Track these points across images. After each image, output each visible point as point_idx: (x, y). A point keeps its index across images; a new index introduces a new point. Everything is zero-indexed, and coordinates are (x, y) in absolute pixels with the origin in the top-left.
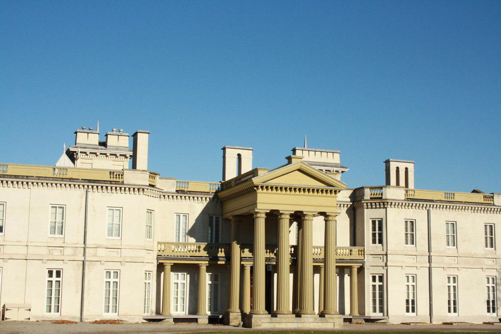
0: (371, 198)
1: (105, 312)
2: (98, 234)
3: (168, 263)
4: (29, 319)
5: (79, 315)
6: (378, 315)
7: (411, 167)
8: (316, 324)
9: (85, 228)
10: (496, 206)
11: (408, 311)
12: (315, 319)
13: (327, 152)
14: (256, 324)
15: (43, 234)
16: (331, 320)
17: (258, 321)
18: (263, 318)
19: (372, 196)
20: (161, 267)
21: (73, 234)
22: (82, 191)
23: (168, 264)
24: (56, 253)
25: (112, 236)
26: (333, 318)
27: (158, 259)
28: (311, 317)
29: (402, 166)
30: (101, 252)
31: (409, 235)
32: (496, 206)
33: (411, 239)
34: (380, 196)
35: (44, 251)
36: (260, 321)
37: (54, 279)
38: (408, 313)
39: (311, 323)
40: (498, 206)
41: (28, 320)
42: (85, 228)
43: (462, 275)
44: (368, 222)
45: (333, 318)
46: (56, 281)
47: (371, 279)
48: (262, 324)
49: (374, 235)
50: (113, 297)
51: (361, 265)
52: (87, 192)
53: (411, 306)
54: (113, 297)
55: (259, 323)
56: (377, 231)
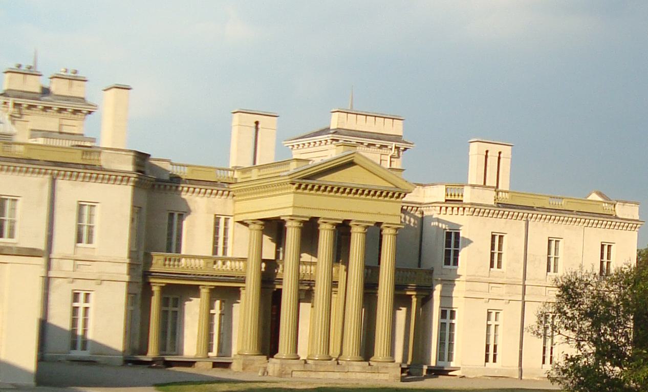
0: (446, 200)
7: (507, 151)
8: (363, 375)
10: (619, 219)
12: (364, 368)
16: (384, 370)
17: (287, 367)
18: (293, 364)
19: (449, 198)
26: (387, 367)
28: (358, 366)
29: (494, 150)
32: (619, 219)
34: (460, 198)
36: (290, 368)
39: (358, 374)
40: (622, 219)
49: (448, 253)
51: (427, 294)
56: (452, 248)
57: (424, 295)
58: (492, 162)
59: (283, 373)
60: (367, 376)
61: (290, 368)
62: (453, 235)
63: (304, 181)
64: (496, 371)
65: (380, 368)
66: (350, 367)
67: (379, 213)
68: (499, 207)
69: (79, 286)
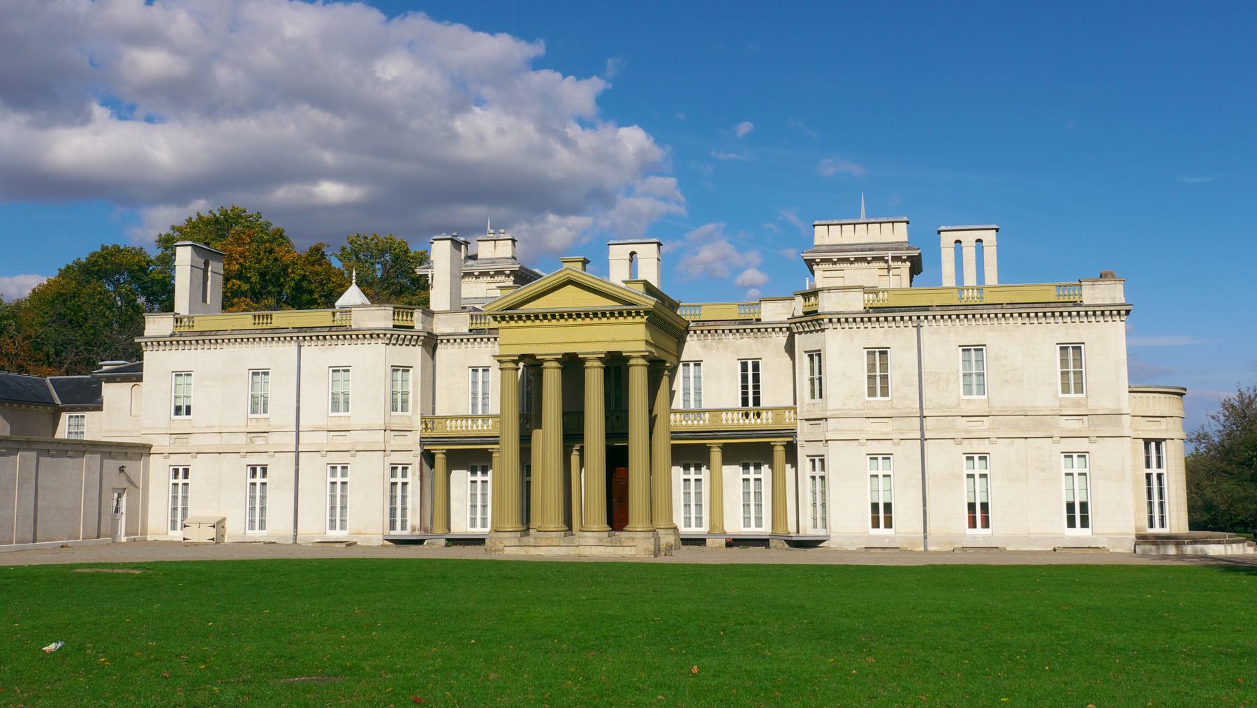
1: (970, 527)
2: (316, 410)
3: (439, 450)
4: (213, 539)
5: (291, 532)
6: (818, 532)
7: (989, 237)
8: (602, 549)
9: (298, 401)
11: (876, 524)
12: (600, 540)
13: (841, 225)
14: (493, 549)
15: (240, 416)
20: (428, 458)
21: (280, 414)
22: (293, 347)
23: (439, 451)
24: (259, 442)
25: (971, 394)
26: (633, 539)
27: (422, 443)
29: (969, 238)
30: (321, 439)
31: (1072, 376)
33: (878, 383)
35: (242, 440)
36: (501, 543)
37: (258, 480)
38: (1072, 529)
41: (212, 541)
42: (298, 401)
43: (997, 451)
44: (801, 357)
45: (633, 539)
46: (755, 480)
47: (809, 464)
48: (506, 548)
50: (337, 510)
52: (300, 347)
53: (882, 514)
54: (337, 510)
55: (501, 546)
57: (784, 441)
58: (969, 253)
59: (493, 549)
60: (607, 551)
61: (501, 543)
62: (816, 359)
63: (504, 312)
64: (887, 540)
65: (623, 539)
66: (581, 539)
67: (614, 341)
68: (868, 312)
69: (175, 460)
